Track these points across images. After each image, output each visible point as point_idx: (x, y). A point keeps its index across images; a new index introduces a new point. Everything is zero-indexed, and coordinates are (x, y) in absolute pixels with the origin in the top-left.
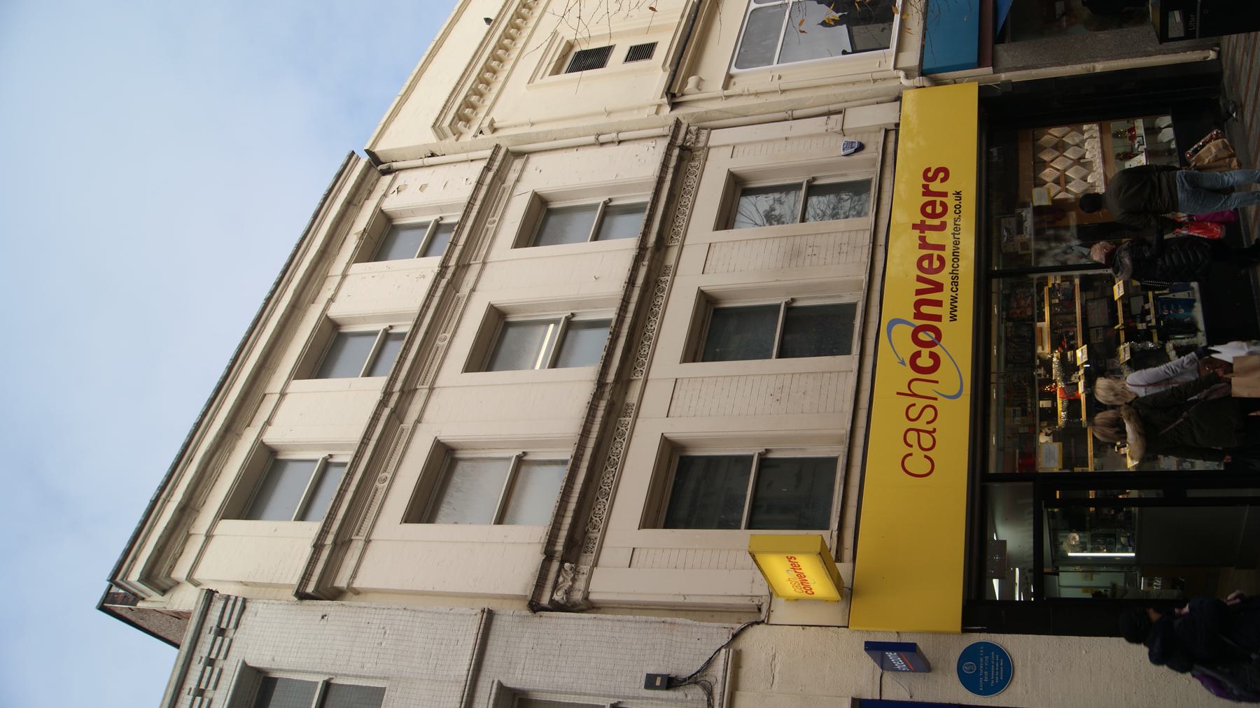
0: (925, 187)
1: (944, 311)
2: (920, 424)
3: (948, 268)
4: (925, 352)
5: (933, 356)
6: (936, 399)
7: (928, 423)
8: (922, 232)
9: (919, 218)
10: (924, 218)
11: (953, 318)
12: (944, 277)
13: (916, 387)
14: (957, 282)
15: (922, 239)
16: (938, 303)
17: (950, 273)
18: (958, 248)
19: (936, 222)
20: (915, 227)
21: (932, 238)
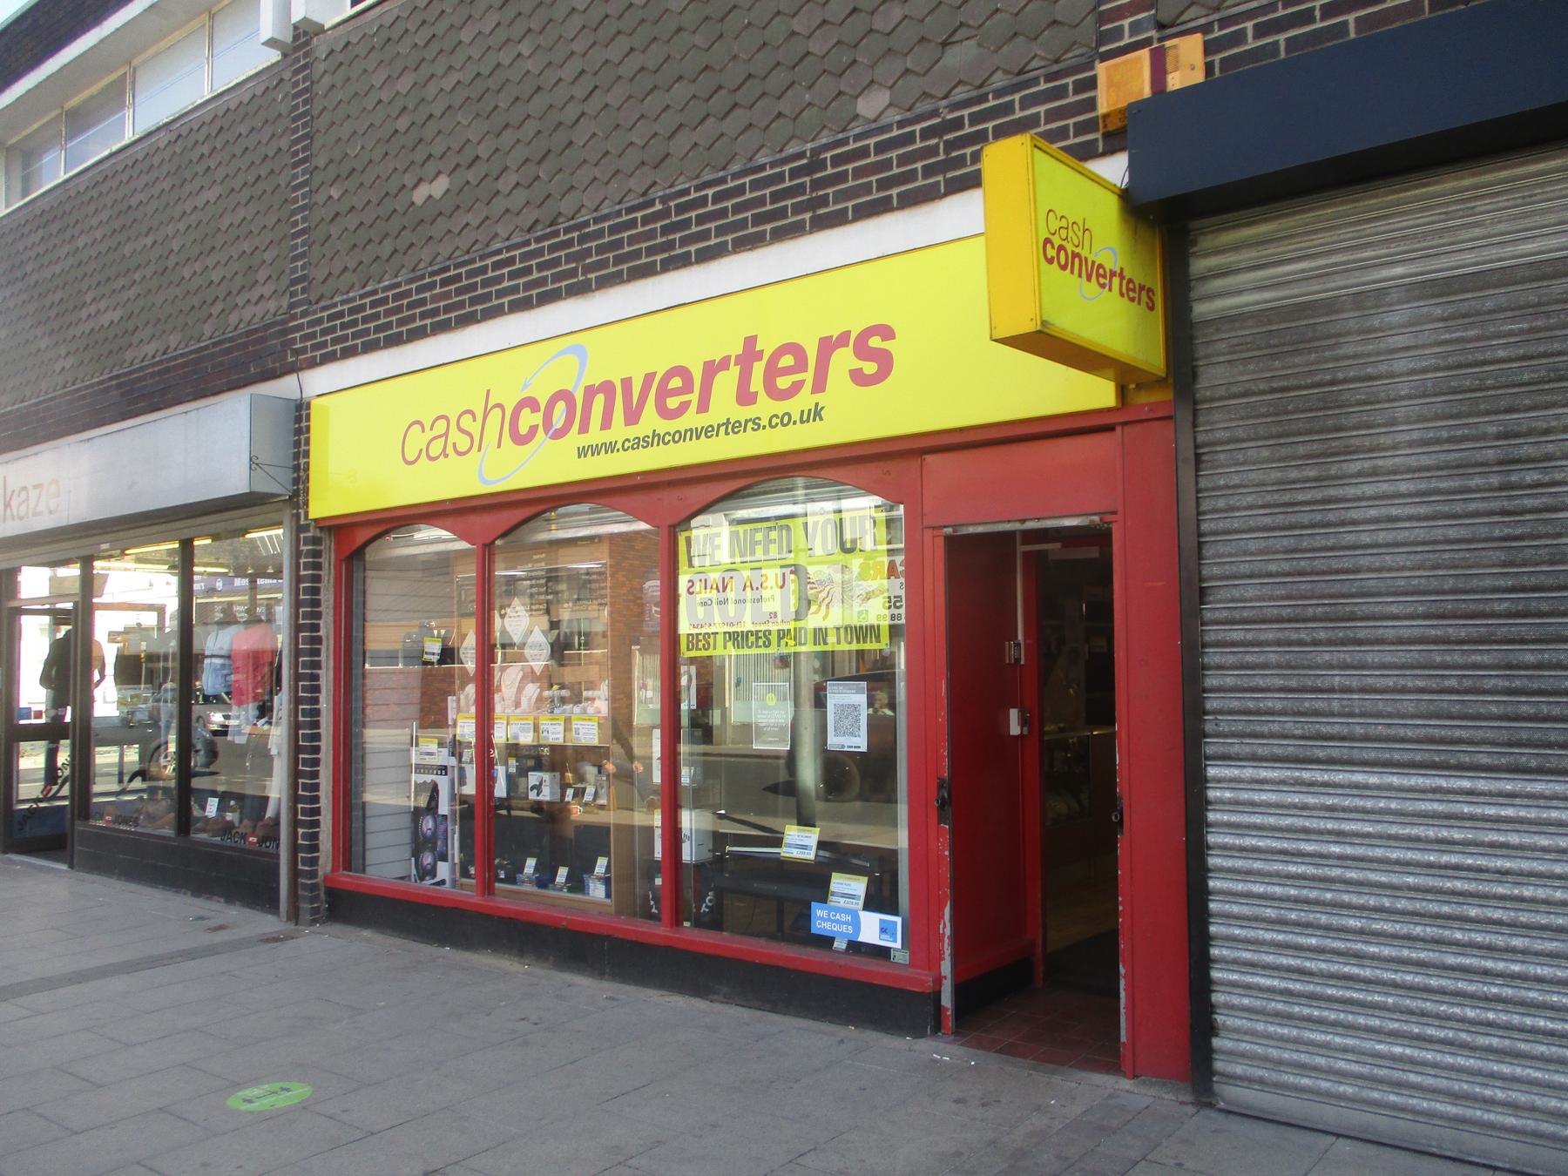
0: (843, 339)
1: (595, 436)
2: (454, 435)
6: (479, 450)
7: (454, 444)
8: (739, 360)
9: (767, 346)
10: (766, 356)
11: (582, 453)
12: (651, 420)
14: (638, 448)
15: (724, 364)
16: (606, 424)
17: (654, 431)
18: (698, 438)
19: (757, 383)
20: (750, 342)
21: (726, 383)
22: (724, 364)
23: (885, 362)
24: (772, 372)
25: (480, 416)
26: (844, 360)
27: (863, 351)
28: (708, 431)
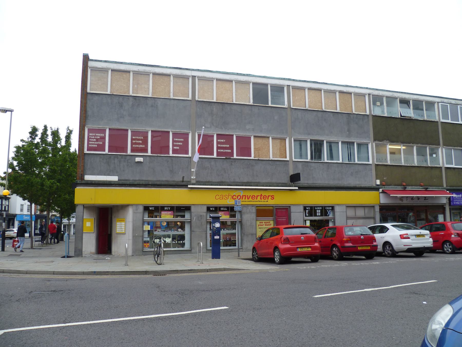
1: (244, 200)
2: (224, 197)
3: (252, 200)
4: (236, 197)
5: (235, 198)
10: (263, 196)
12: (250, 199)
13: (230, 196)
15: (259, 196)
16: (245, 199)
20: (261, 194)
21: (259, 198)
22: (259, 196)
23: (274, 198)
24: (263, 197)
25: (228, 196)
26: (270, 197)
27: (272, 197)
28: (257, 201)
